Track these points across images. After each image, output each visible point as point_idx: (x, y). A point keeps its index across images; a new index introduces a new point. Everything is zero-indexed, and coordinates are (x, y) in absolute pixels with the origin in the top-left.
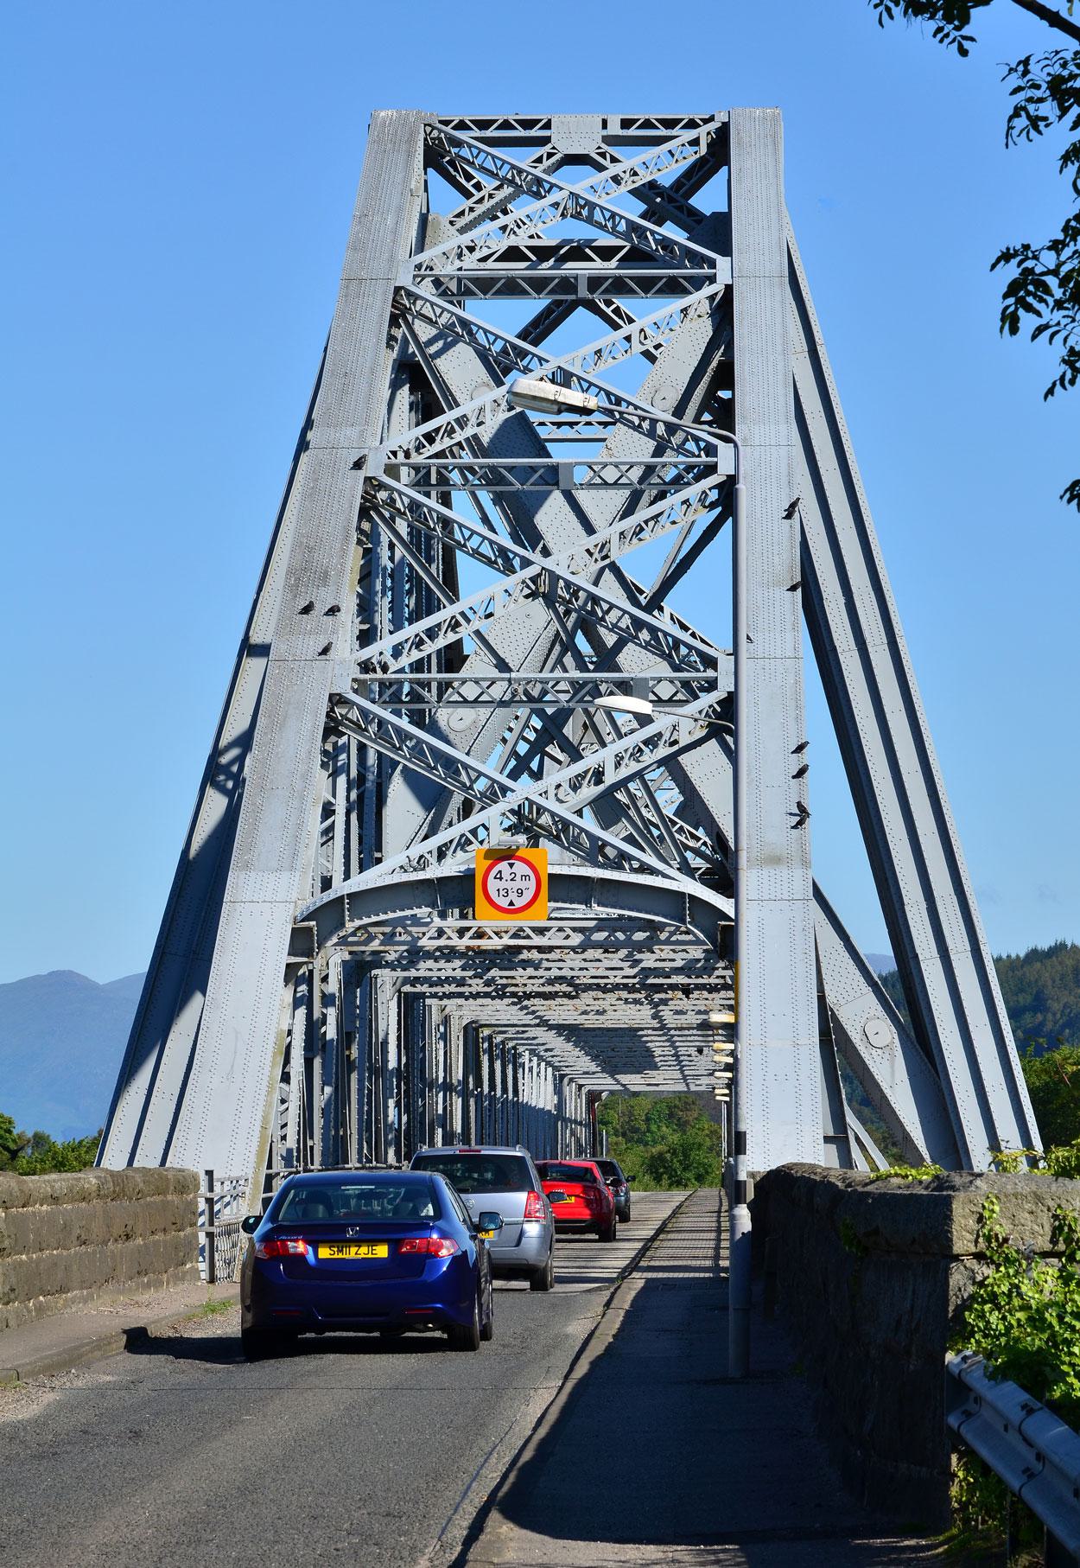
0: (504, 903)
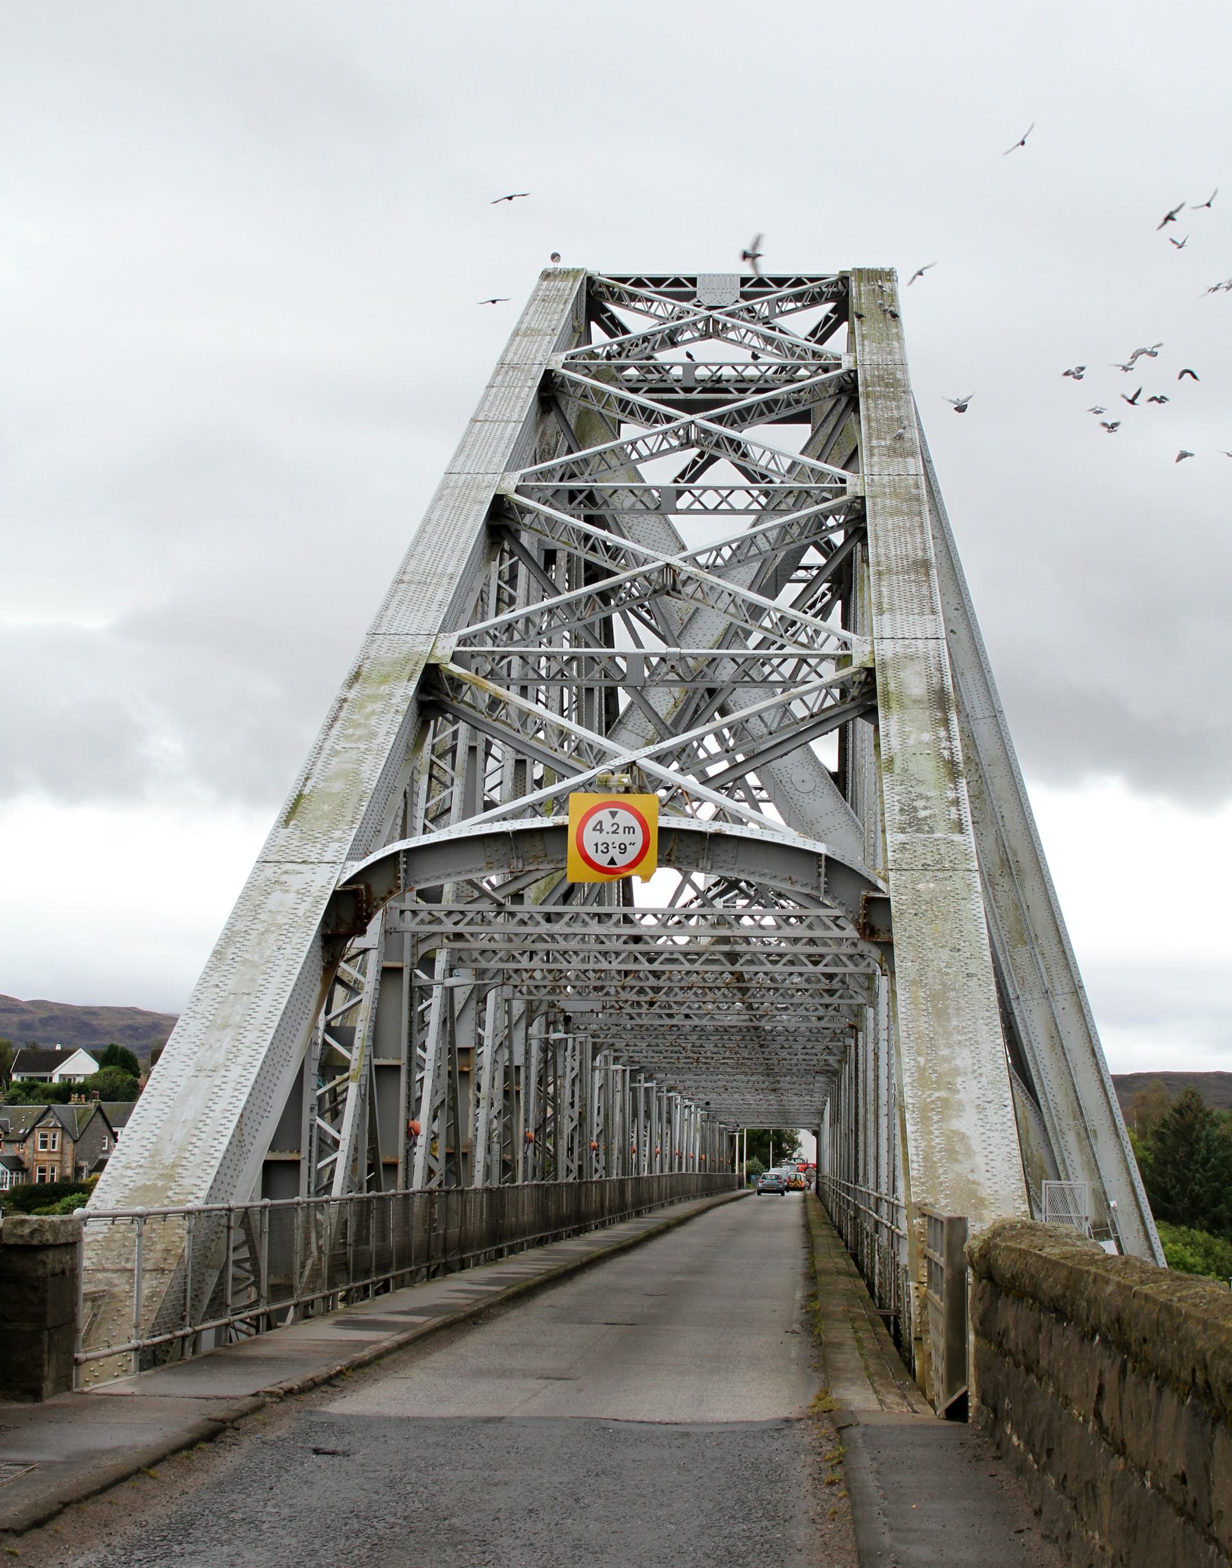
0: (602, 860)
